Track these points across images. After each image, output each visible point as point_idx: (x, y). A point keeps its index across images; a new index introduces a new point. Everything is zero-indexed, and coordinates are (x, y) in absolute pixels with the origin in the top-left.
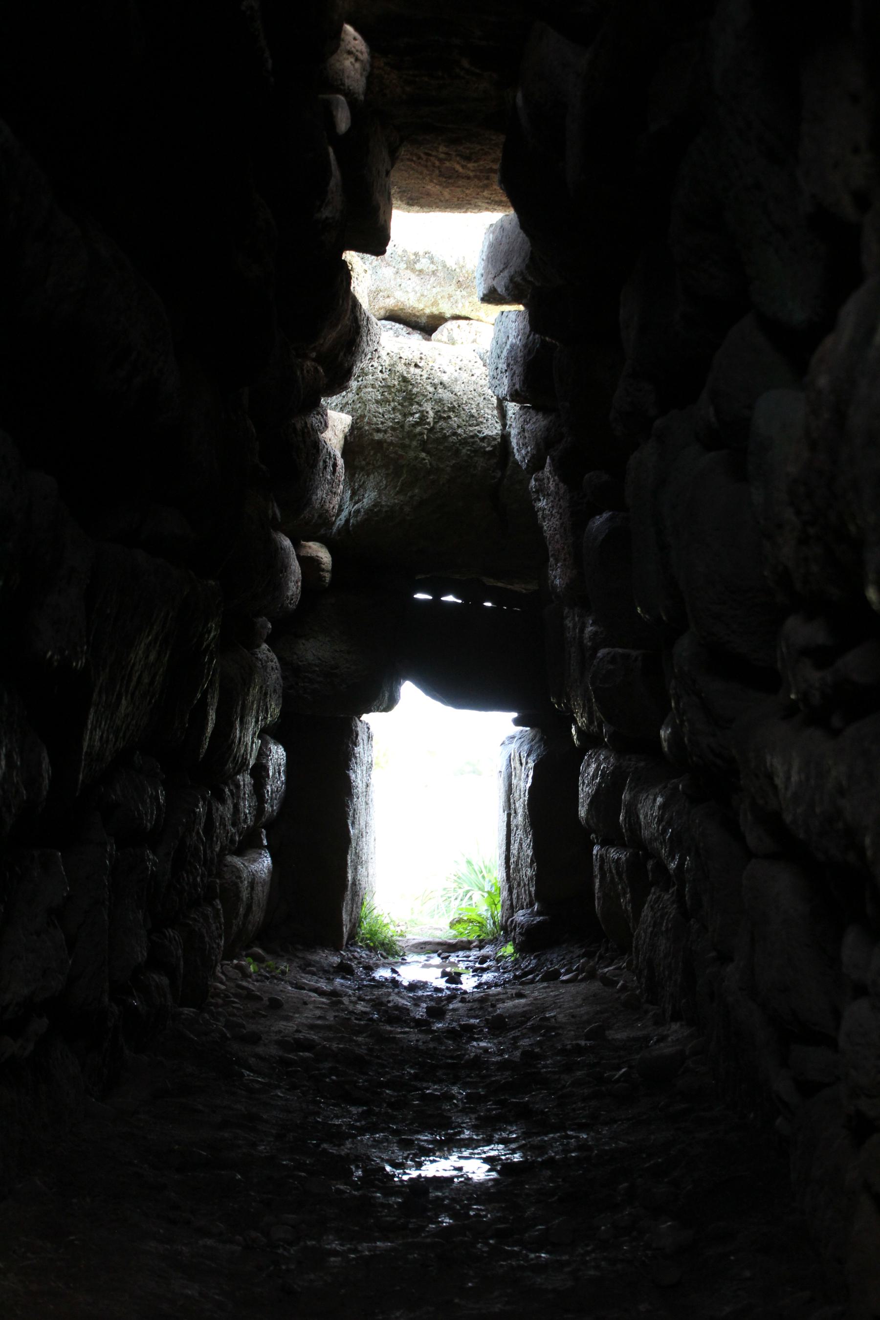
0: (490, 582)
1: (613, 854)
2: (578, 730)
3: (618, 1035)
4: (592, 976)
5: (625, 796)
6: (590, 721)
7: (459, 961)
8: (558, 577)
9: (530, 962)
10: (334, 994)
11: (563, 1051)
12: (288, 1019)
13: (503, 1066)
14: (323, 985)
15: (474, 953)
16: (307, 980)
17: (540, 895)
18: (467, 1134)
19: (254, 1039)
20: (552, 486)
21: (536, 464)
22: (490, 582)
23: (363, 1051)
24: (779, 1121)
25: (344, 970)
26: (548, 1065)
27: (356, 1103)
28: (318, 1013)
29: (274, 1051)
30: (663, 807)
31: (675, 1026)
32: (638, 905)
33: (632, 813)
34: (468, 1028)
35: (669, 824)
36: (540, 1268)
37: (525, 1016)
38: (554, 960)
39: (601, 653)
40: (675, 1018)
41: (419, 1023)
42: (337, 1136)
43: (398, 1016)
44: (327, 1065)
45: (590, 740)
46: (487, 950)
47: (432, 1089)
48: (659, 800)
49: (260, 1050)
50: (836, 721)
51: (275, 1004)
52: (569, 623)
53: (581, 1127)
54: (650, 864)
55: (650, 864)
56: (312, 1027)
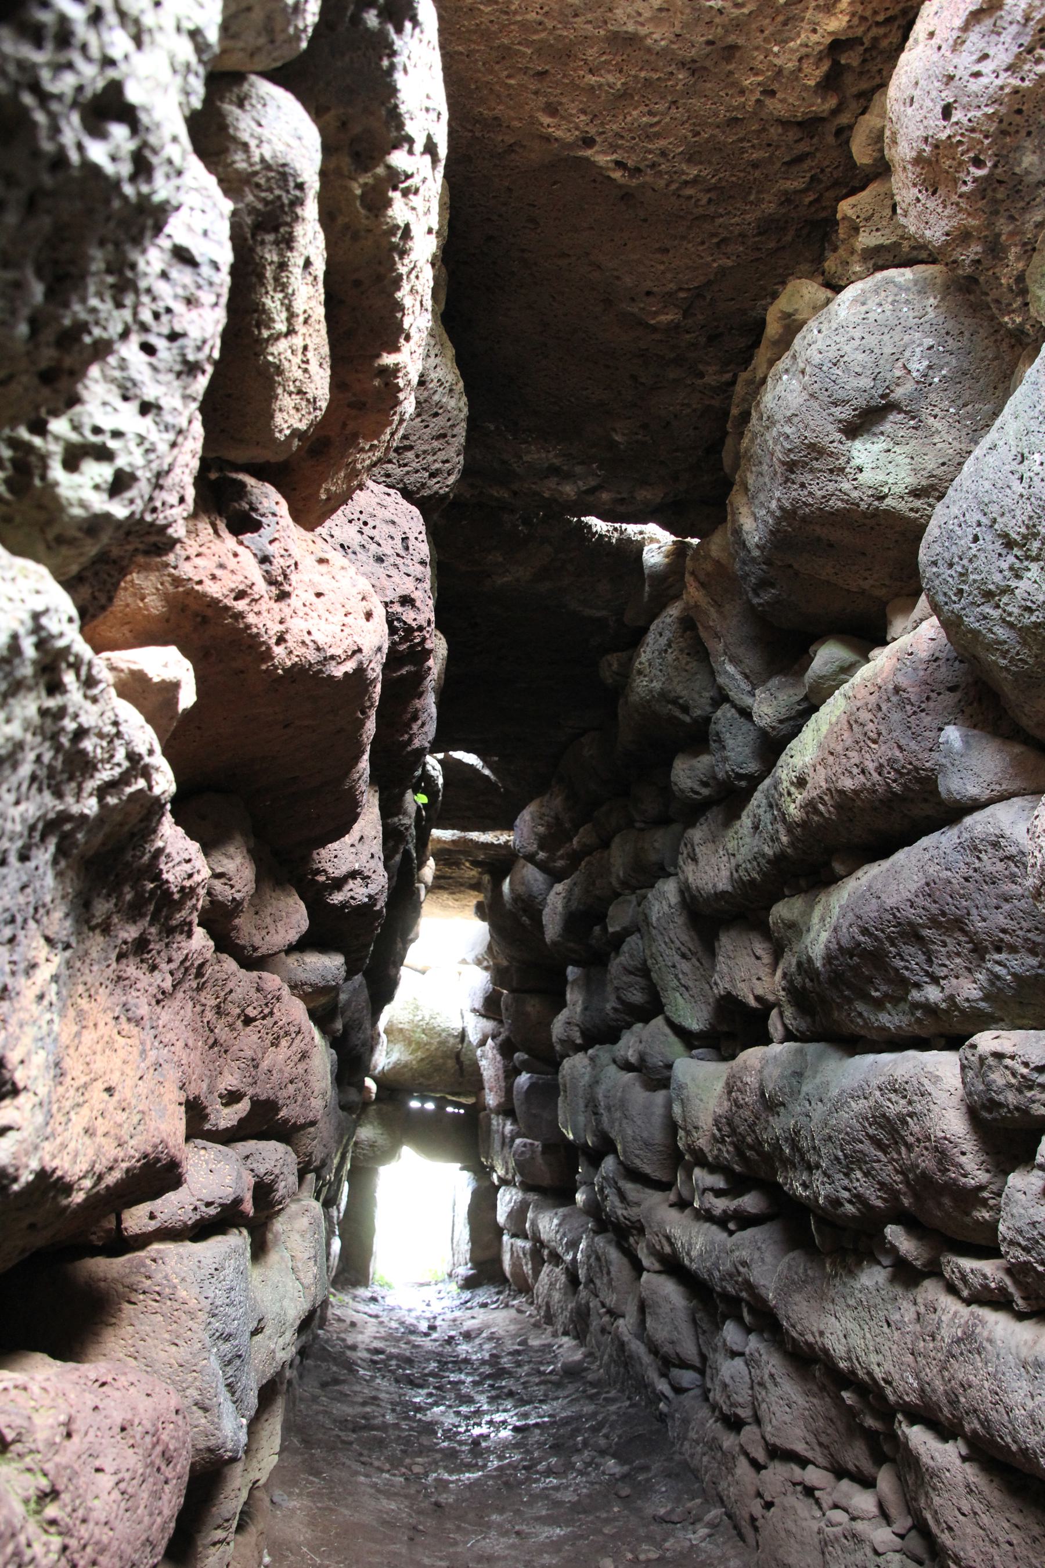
0: (450, 1098)
1: (520, 1243)
2: (499, 1177)
3: (534, 1342)
4: (507, 1306)
5: (530, 1215)
6: (507, 1173)
7: (430, 1293)
8: (491, 1099)
9: (467, 1295)
10: (377, 1316)
11: (510, 1354)
12: (362, 1333)
13: (483, 1362)
14: (367, 1309)
15: (434, 1289)
16: (361, 1307)
17: (471, 1260)
18: (485, 1407)
19: (354, 1348)
20: (490, 1055)
21: (483, 1043)
22: (450, 1098)
23: (408, 1353)
24: (661, 1405)
25: (374, 1299)
26: (506, 1362)
27: (421, 1387)
28: (375, 1329)
29: (366, 1355)
30: (560, 1225)
31: (565, 1339)
32: (536, 1273)
33: (534, 1224)
34: (452, 1338)
35: (564, 1235)
36: (556, 1488)
37: (480, 1331)
38: (484, 1295)
39: (518, 1141)
40: (565, 1333)
41: (426, 1335)
42: (419, 1409)
43: (413, 1331)
44: (394, 1362)
45: (504, 1182)
46: (440, 1286)
47: (453, 1377)
48: (556, 1221)
49: (359, 1354)
50: (732, 1226)
51: (353, 1324)
52: (494, 1122)
53: (541, 1401)
54: (546, 1252)
55: (546, 1252)
56: (375, 1338)
